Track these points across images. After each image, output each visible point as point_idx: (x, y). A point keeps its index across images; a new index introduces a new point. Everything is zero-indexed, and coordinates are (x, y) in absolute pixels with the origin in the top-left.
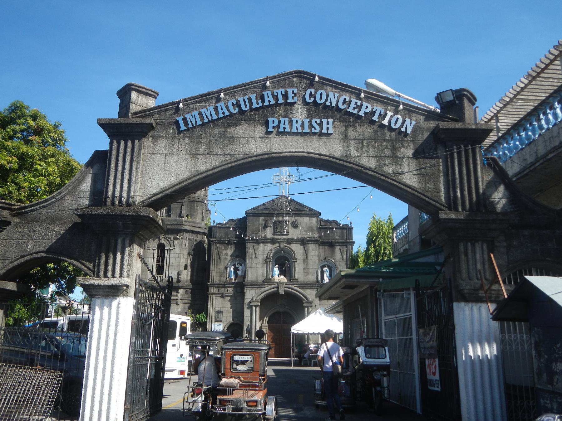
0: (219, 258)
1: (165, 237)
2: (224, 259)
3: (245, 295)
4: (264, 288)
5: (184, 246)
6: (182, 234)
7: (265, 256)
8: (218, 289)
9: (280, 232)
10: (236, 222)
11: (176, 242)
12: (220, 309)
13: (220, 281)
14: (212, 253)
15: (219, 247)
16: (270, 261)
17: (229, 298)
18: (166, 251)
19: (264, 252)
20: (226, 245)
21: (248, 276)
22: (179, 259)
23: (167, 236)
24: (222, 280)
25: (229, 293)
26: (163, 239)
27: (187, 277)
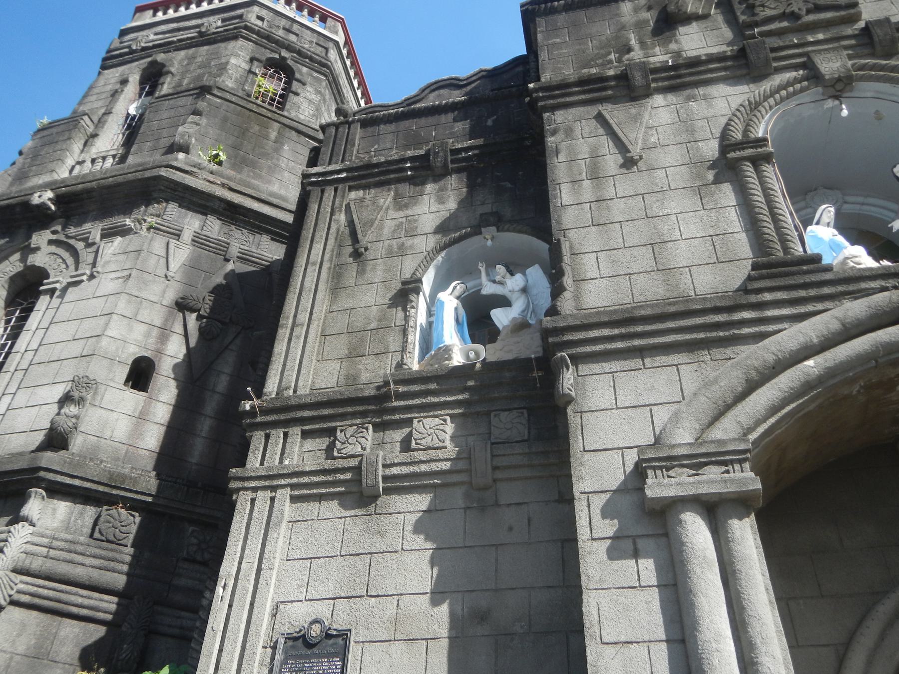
0: (357, 255)
1: (62, 237)
2: (390, 250)
3: (573, 419)
4: (763, 336)
5: (154, 263)
6: (155, 208)
7: (711, 149)
8: (323, 443)
9: (783, 16)
10: (469, 88)
12: (323, 610)
13: (352, 379)
15: (362, 200)
16: (757, 161)
17: (421, 502)
19: (691, 131)
20: (405, 188)
21: (578, 281)
23: (72, 231)
24: (364, 377)
25: (422, 456)
26: (46, 249)
27: (137, 431)
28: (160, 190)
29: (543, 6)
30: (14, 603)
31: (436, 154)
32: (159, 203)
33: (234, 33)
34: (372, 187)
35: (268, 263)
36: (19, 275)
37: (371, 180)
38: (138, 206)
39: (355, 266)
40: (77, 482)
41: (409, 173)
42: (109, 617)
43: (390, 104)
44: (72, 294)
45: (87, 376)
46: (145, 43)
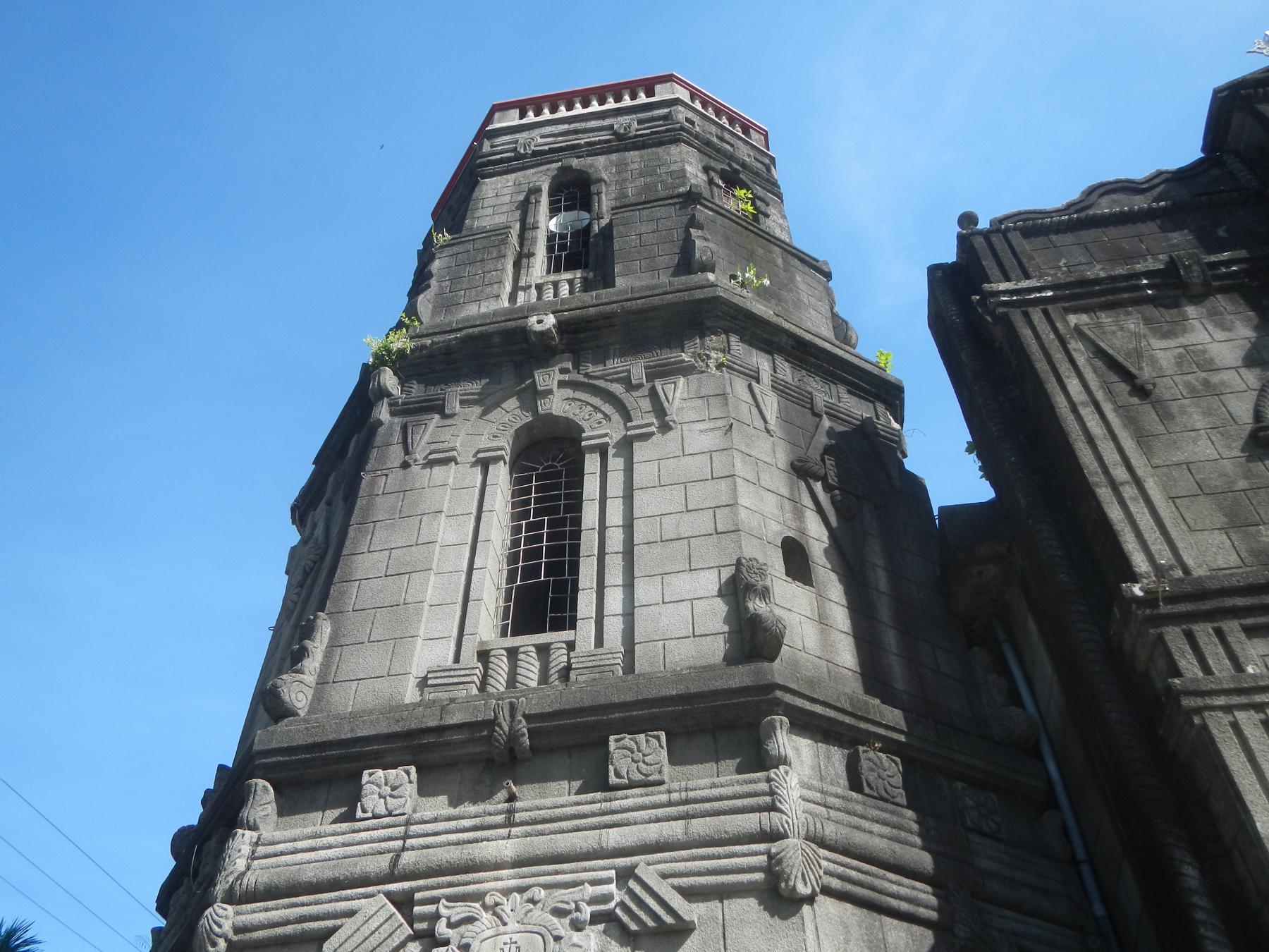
0: (1141, 391)
1: (581, 378)
6: (713, 341)
11: (677, 393)
14: (1042, 366)
18: (592, 464)
22: (723, 485)
27: (826, 642)
28: (718, 316)
29: (1261, 90)
30: (827, 891)
31: (1186, 268)
32: (716, 334)
33: (671, 135)
34: (1097, 309)
35: (858, 423)
36: (527, 428)
37: (1096, 300)
38: (691, 338)
39: (1148, 407)
40: (818, 709)
41: (1150, 292)
42: (933, 915)
43: (1048, 210)
44: (641, 451)
45: (755, 559)
46: (535, 146)
